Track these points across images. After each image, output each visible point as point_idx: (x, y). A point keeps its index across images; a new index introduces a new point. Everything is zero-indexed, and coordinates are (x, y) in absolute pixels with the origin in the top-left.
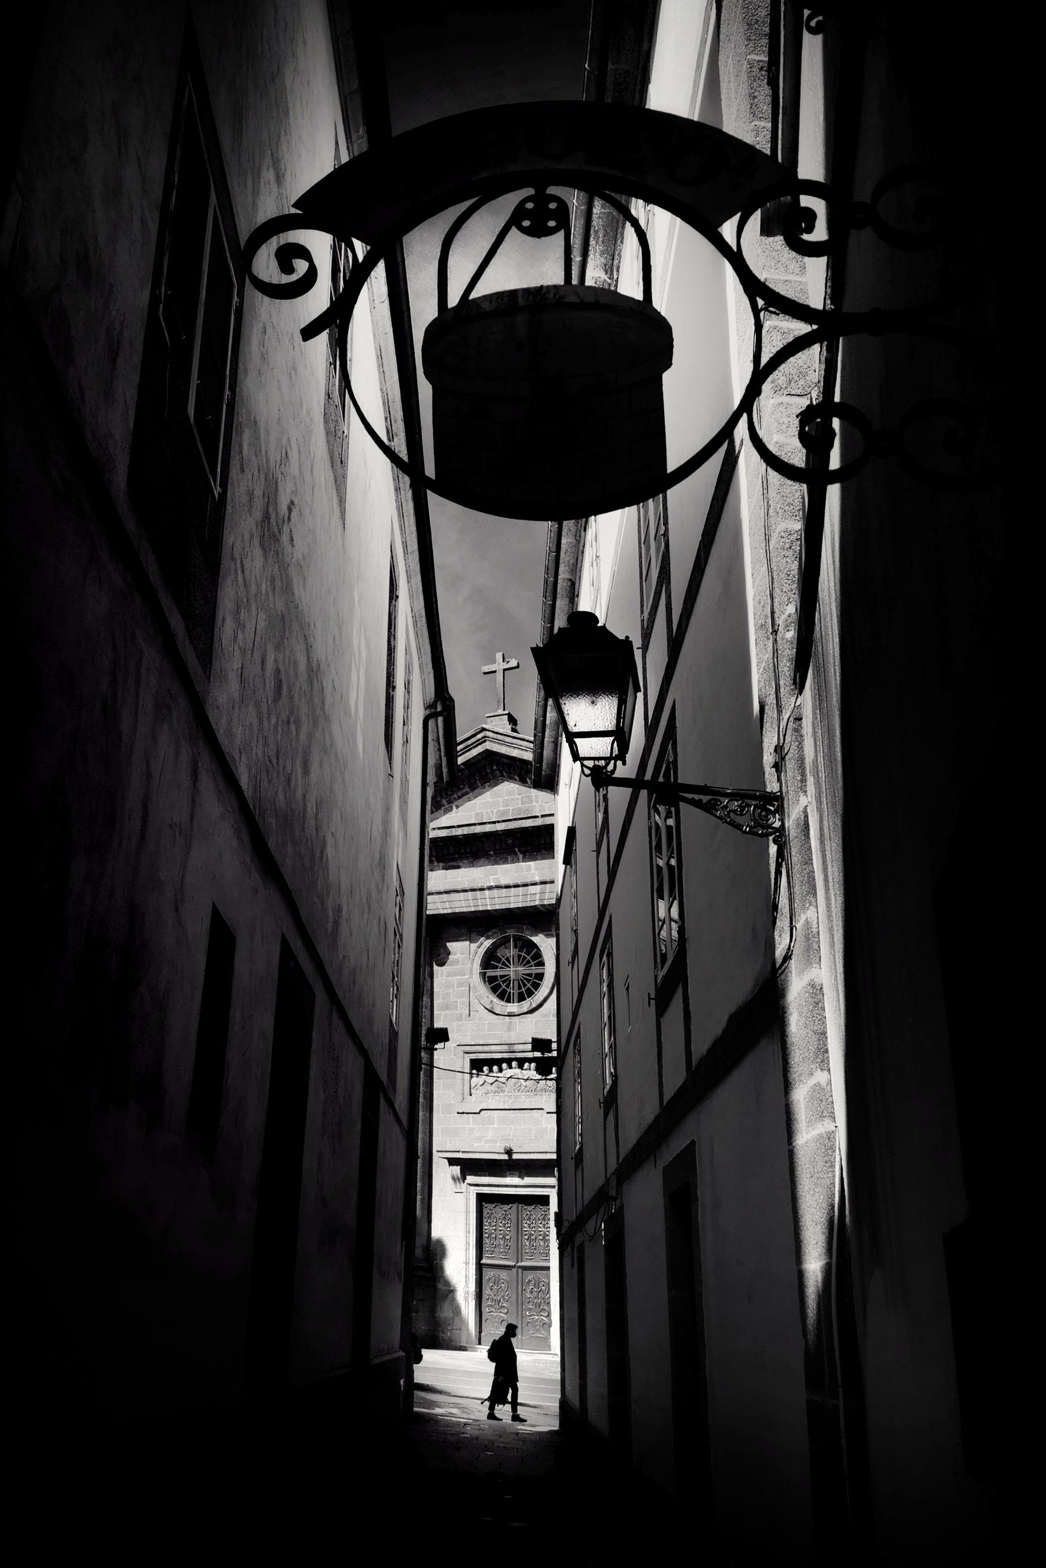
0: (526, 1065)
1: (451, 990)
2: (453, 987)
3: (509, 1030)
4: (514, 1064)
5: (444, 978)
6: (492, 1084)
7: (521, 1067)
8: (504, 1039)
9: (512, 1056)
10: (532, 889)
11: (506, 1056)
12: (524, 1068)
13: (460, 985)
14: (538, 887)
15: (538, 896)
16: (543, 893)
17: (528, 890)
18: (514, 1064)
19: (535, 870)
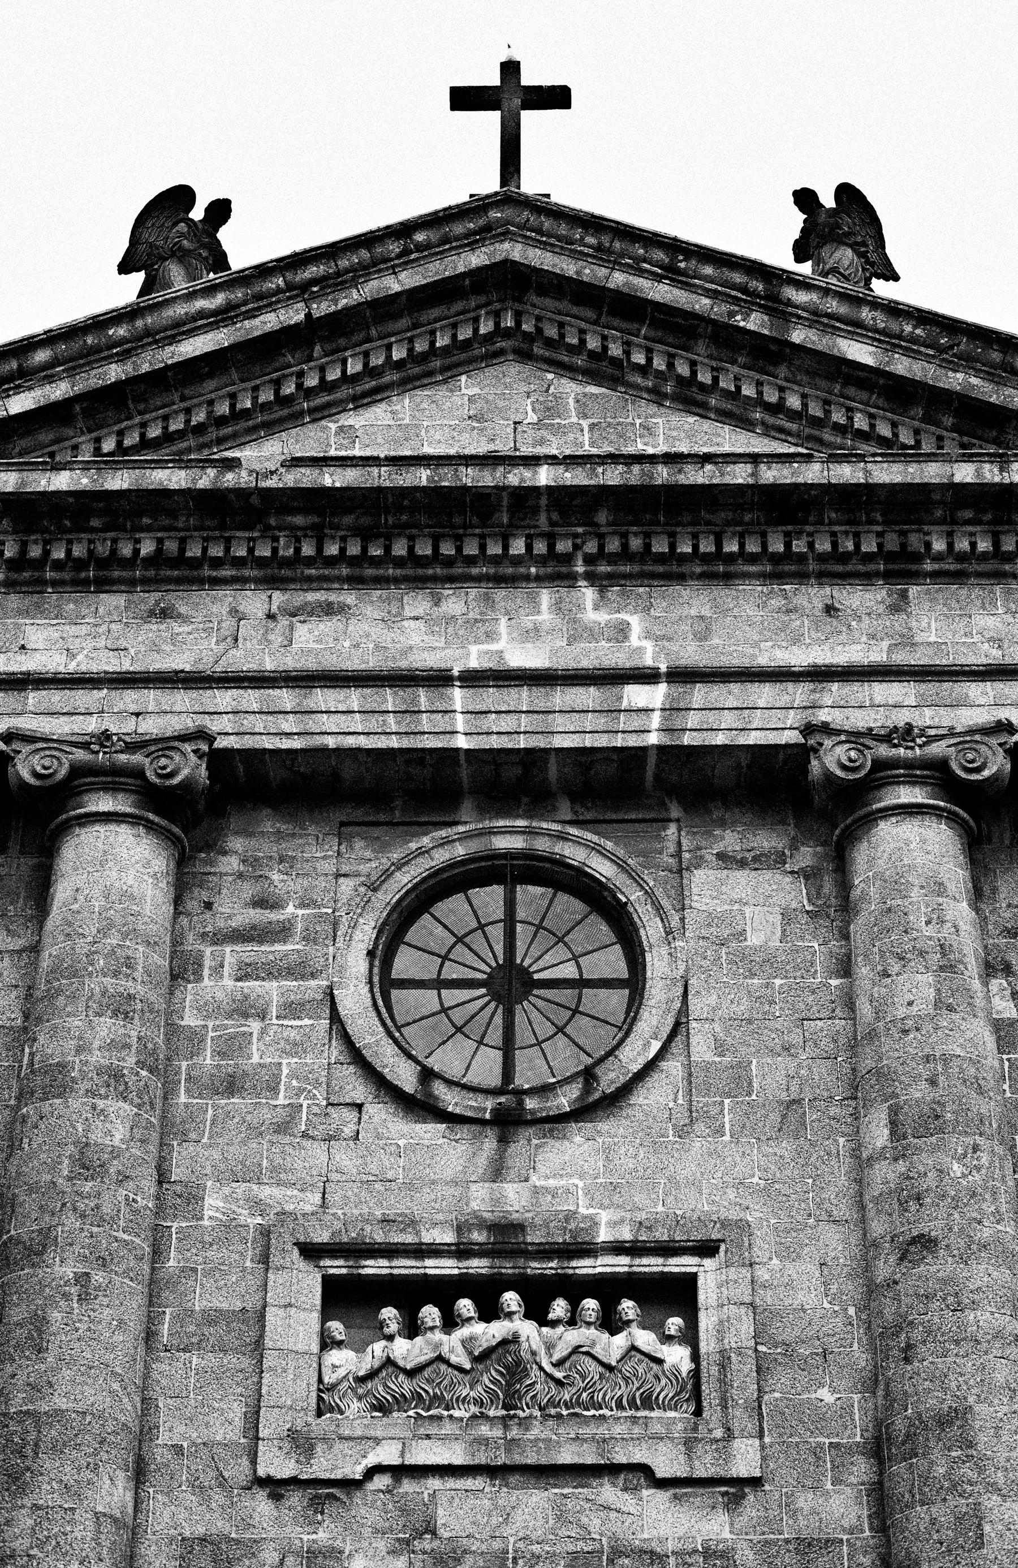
0: (559, 1308)
1: (255, 1026)
2: (263, 1016)
3: (497, 1172)
4: (511, 1299)
5: (228, 982)
6: (412, 1373)
7: (537, 1313)
8: (474, 1205)
9: (508, 1268)
10: (636, 695)
11: (478, 1266)
12: (551, 1316)
13: (292, 1009)
14: (662, 688)
15: (656, 720)
16: (671, 710)
17: (620, 698)
18: (511, 1299)
19: (648, 635)
